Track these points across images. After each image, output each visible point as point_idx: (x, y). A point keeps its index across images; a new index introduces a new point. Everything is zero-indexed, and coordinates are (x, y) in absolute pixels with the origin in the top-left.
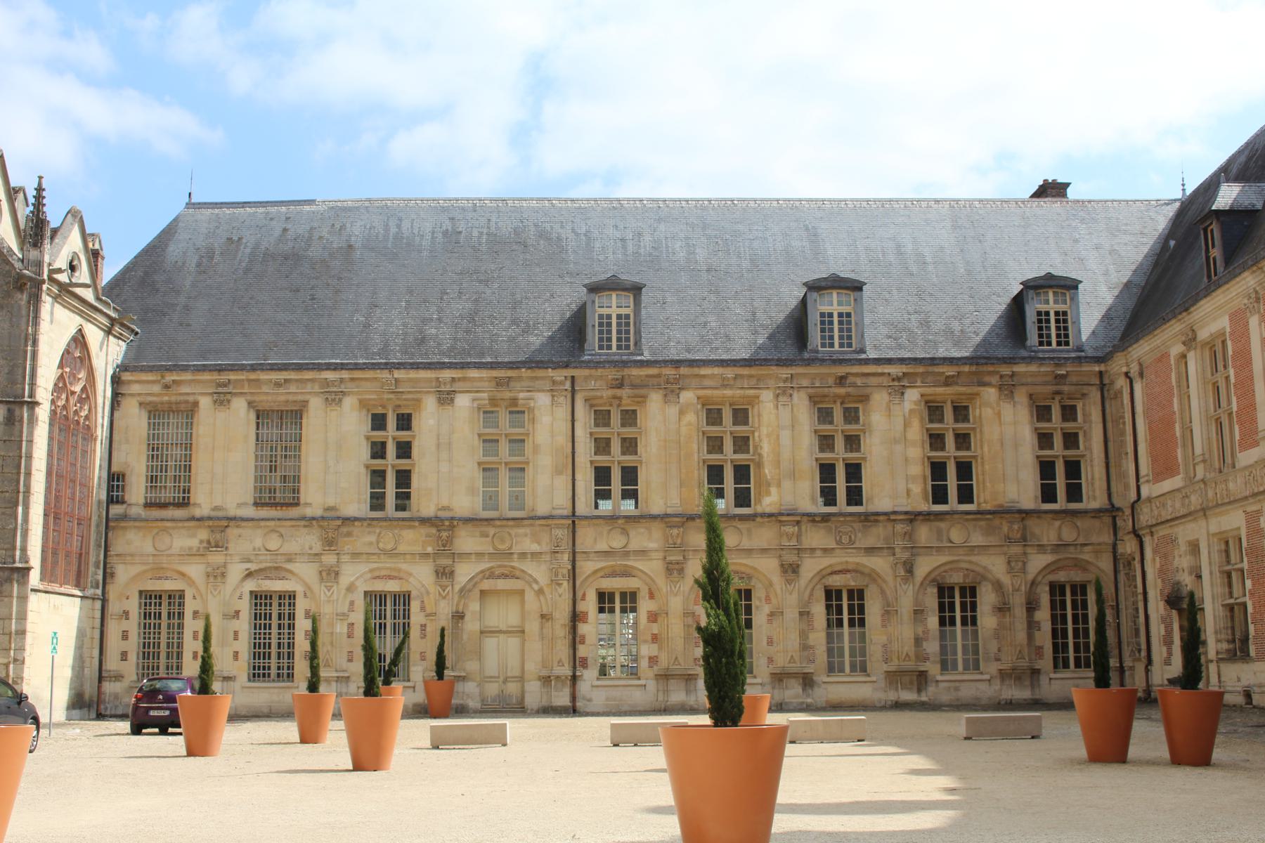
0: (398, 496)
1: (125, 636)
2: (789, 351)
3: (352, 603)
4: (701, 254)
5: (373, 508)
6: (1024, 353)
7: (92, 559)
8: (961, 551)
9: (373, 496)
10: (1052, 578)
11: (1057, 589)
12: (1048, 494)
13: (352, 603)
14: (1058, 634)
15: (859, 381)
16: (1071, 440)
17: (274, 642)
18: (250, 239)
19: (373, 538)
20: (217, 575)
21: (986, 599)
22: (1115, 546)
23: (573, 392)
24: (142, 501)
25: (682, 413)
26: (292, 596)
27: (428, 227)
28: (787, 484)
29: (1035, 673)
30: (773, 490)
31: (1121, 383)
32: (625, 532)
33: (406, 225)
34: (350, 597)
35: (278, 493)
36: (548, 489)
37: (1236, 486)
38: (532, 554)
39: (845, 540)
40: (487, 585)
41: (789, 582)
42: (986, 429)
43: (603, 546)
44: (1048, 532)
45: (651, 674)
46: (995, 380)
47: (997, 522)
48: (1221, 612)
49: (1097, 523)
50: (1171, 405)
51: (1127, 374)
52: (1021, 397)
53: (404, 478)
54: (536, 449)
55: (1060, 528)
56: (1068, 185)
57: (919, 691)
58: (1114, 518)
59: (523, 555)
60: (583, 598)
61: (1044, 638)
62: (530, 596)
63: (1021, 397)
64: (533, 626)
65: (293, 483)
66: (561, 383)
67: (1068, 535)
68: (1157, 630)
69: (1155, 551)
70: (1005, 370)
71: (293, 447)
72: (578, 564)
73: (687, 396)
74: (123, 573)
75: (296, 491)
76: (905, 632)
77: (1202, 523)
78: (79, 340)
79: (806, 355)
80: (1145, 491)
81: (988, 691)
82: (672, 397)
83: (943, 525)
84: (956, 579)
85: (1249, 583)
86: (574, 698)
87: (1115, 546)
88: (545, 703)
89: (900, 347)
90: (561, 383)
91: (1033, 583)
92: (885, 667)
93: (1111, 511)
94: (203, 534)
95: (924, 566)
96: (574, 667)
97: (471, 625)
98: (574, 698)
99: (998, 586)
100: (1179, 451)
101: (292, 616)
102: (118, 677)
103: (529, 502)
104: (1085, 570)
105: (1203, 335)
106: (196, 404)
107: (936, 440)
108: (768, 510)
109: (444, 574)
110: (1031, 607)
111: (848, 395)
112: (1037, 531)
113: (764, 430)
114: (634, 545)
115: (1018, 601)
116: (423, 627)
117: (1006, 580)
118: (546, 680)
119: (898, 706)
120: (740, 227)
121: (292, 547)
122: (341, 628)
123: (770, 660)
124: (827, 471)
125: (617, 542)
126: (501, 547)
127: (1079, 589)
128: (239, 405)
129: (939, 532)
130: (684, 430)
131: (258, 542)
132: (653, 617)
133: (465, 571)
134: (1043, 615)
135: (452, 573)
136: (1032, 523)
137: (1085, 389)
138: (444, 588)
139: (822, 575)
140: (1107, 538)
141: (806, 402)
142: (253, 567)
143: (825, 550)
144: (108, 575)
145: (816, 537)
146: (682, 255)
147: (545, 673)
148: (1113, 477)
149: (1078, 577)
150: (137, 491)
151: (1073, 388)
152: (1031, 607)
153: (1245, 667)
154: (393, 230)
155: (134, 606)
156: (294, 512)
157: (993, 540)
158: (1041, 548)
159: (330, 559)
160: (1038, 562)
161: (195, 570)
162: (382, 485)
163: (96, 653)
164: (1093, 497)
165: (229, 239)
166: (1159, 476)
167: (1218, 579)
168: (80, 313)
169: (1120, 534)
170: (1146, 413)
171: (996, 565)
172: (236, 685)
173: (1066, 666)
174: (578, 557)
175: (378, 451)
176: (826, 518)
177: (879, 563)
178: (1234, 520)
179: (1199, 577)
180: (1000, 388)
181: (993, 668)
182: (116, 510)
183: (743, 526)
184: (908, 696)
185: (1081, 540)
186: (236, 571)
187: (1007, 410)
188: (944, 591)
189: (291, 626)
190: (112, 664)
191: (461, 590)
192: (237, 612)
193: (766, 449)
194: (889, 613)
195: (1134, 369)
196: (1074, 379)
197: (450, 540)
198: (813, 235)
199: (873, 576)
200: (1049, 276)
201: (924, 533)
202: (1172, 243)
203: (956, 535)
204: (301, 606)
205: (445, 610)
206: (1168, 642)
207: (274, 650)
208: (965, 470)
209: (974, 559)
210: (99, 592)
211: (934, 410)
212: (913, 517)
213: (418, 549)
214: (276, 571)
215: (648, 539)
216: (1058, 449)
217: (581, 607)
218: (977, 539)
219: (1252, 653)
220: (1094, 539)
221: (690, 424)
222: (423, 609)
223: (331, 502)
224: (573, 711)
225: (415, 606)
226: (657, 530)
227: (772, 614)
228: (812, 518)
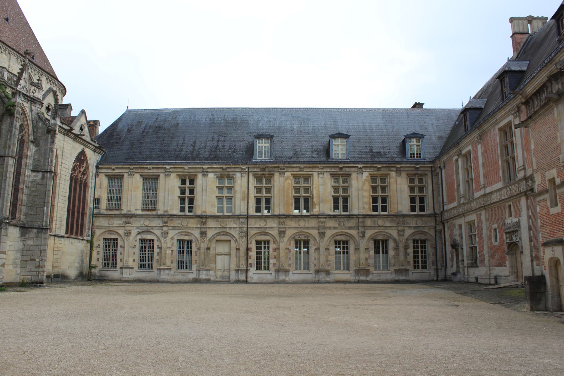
0: (189, 207)
1: (98, 253)
2: (324, 159)
3: (173, 243)
4: (296, 127)
5: (181, 211)
6: (405, 160)
7: (87, 227)
8: (382, 228)
9: (181, 207)
10: (414, 238)
11: (415, 241)
12: (413, 209)
13: (173, 243)
14: (415, 257)
15: (347, 169)
16: (421, 190)
17: (147, 256)
19: (180, 222)
20: (128, 233)
21: (391, 244)
22: (435, 227)
23: (249, 172)
24: (105, 208)
25: (286, 180)
26: (153, 240)
27: (204, 117)
28: (321, 204)
29: (407, 270)
30: (317, 207)
31: (438, 170)
33: (197, 117)
37: (474, 205)
38: (233, 228)
39: (342, 224)
40: (218, 238)
41: (322, 238)
42: (392, 186)
43: (257, 225)
44: (413, 222)
45: (273, 269)
46: (394, 169)
47: (395, 218)
48: (469, 250)
49: (429, 218)
50: (453, 176)
51: (440, 167)
52: (404, 174)
53: (191, 201)
54: (235, 192)
55: (416, 221)
56: (423, 104)
57: (367, 276)
58: (436, 217)
59: (230, 228)
60: (251, 243)
61: (411, 258)
62: (232, 242)
63: (404, 174)
64: (233, 252)
65: (155, 202)
66: (245, 169)
67: (420, 223)
68: (449, 256)
69: (448, 228)
70: (398, 166)
71: (155, 191)
72: (249, 231)
73: (287, 174)
74: (98, 232)
75: (155, 205)
76: (362, 256)
77: (463, 218)
78: (82, 153)
79: (329, 160)
80: (446, 208)
81: (390, 277)
82: (282, 175)
83: (376, 219)
84: (380, 237)
85: (477, 239)
86: (247, 277)
87: (435, 227)
88: (237, 279)
89: (362, 158)
90: (245, 169)
91: (407, 239)
92: (355, 268)
93: (434, 215)
94: (124, 219)
95: (369, 233)
96: (247, 267)
97: (212, 252)
98: (247, 277)
99: (395, 240)
100: (456, 193)
101: (153, 248)
102: (95, 267)
103: (233, 210)
104: (425, 235)
105: (464, 152)
106: (123, 175)
107: (374, 189)
108: (315, 214)
109: (203, 234)
110: (406, 248)
111: (343, 174)
112: (409, 221)
113: (314, 186)
114: (267, 226)
115: (401, 245)
117: (397, 238)
118: (237, 271)
119: (359, 282)
120: (310, 117)
122: (169, 252)
123: (315, 265)
124: (336, 200)
125: (262, 224)
126: (223, 225)
127: (424, 242)
128: (137, 176)
129: (374, 221)
130: (286, 186)
131: (142, 222)
132: (275, 250)
133: (210, 234)
134: (410, 250)
135: (206, 234)
136: (406, 219)
137: (426, 172)
138: (203, 239)
139: (334, 236)
140: (433, 224)
141: (329, 176)
142: (140, 231)
143: (334, 227)
144: (93, 233)
145: (331, 223)
146: (289, 127)
147: (237, 268)
148: (435, 203)
149: (423, 237)
150: (104, 204)
151: (422, 172)
152: (406, 248)
153: (476, 269)
154: (193, 118)
155: (102, 243)
156: (154, 213)
157: (393, 225)
158: (410, 227)
159: (165, 229)
160: (408, 232)
162: (184, 204)
163: (88, 259)
164: (429, 210)
165: (139, 121)
166: (450, 202)
167: (468, 238)
168: (83, 145)
169: (437, 223)
170: (446, 180)
171: (394, 233)
172: (134, 270)
173: (418, 268)
174: (249, 229)
175: (183, 192)
176: (335, 216)
177: (354, 232)
178: (473, 217)
179: (462, 237)
180: (396, 172)
181: (392, 269)
182: (96, 211)
183: (306, 219)
184: (362, 278)
185: (424, 225)
186: (134, 232)
187: (399, 179)
188: (376, 242)
189: (153, 251)
190: (94, 262)
191: (209, 240)
192: (135, 246)
193: (315, 192)
194: (357, 249)
195: (442, 165)
196: (422, 169)
197: (205, 223)
198: (335, 121)
199: (351, 236)
200: (414, 134)
201: (369, 222)
202: (457, 123)
203: (380, 222)
204: (156, 244)
205: (203, 246)
206: (452, 260)
207: (147, 259)
208: (384, 200)
209: (386, 231)
210: (90, 238)
211: (374, 178)
212: (365, 216)
214: (148, 232)
216: (417, 193)
217: (250, 246)
218: (387, 224)
219: (478, 264)
220: (429, 224)
221: (288, 183)
222: (196, 246)
223: (166, 209)
224: (246, 282)
225: (194, 245)
226: (276, 220)
227: (316, 249)
228: (331, 217)
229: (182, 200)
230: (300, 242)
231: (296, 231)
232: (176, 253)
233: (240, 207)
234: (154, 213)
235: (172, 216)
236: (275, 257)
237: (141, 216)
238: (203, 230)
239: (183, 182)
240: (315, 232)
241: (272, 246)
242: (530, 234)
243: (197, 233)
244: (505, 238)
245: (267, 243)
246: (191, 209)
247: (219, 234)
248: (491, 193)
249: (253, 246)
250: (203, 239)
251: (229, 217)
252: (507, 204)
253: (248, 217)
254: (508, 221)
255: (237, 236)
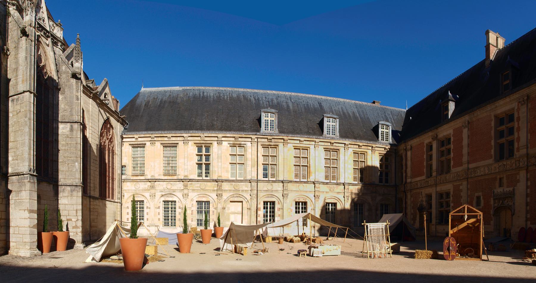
0: (206, 173)
3: (192, 204)
5: (199, 176)
13: (192, 204)
18: (160, 97)
32: (272, 185)
34: (192, 203)
35: (170, 171)
36: (252, 171)
40: (232, 199)
59: (243, 191)
65: (174, 168)
71: (174, 158)
97: (226, 211)
116: (213, 212)
121: (174, 188)
128: (158, 144)
131: (165, 186)
133: (225, 196)
156: (175, 177)
159: (186, 191)
161: (147, 195)
205: (220, 206)
213: (212, 189)
215: (279, 187)
222: (213, 206)
223: (186, 174)
228: (324, 183)
229: (200, 165)
230: (299, 203)
231: (297, 194)
232: (195, 212)
233: (251, 173)
234: (175, 177)
235: (191, 180)
236: (279, 215)
237: (164, 180)
238: (219, 192)
239: (200, 150)
240: (311, 196)
241: (277, 206)
242: (526, 200)
243: (214, 195)
244: (492, 202)
245: (273, 203)
246: (207, 173)
247: (232, 196)
248: (477, 168)
249: (261, 206)
250: (220, 200)
251: (241, 181)
252: (498, 177)
253: (257, 181)
254: (499, 190)
255: (249, 198)
